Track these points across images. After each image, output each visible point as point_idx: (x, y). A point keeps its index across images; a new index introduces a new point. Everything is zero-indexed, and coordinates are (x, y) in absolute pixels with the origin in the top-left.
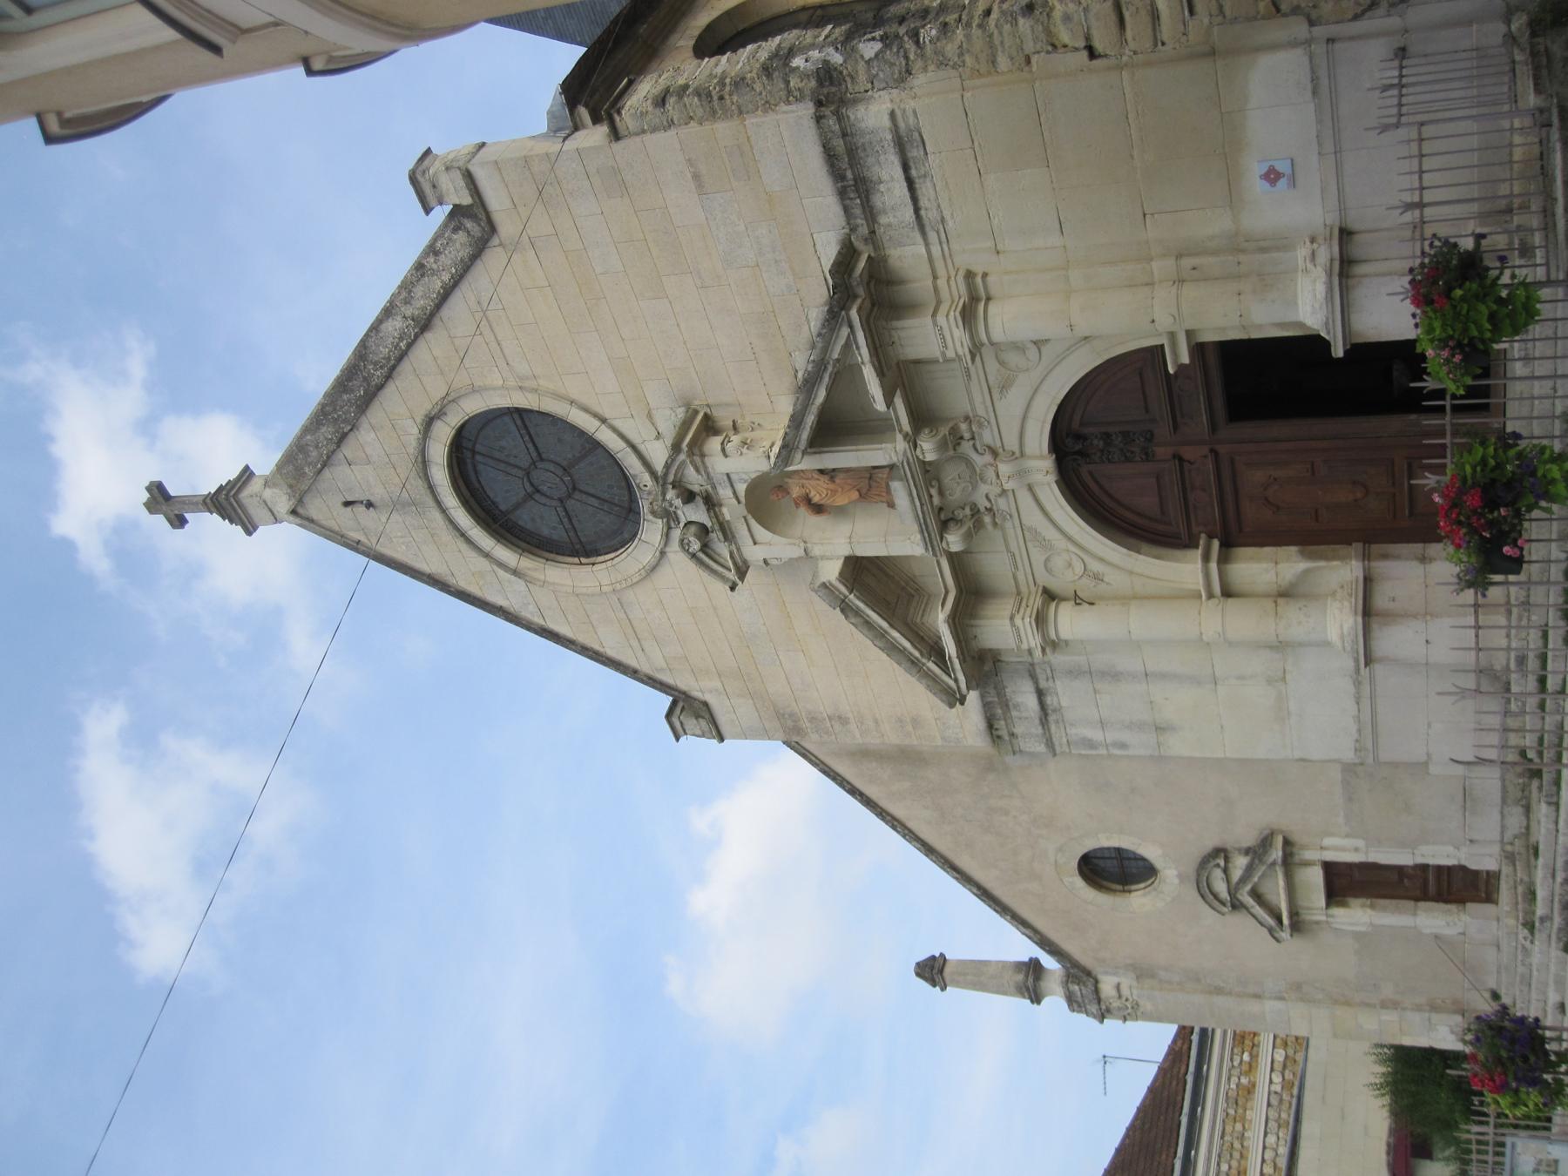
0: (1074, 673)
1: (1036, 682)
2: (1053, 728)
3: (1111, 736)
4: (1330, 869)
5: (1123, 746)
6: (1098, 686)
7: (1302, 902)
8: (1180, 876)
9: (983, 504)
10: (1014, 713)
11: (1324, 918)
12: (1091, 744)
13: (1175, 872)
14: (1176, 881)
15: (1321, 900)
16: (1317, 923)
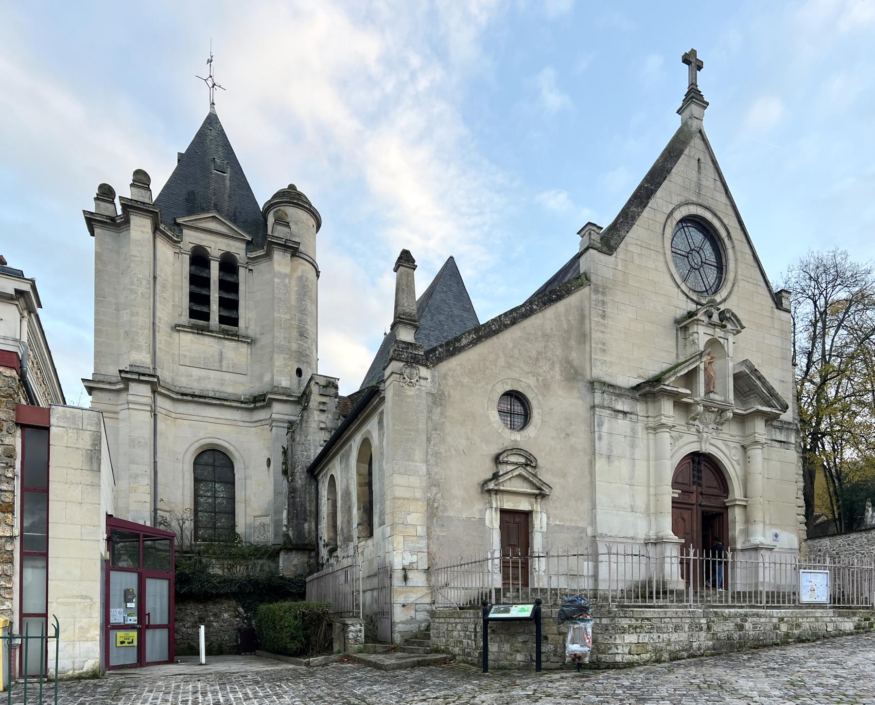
0: (633, 430)
1: (631, 413)
2: (609, 412)
3: (605, 436)
4: (527, 515)
5: (600, 438)
6: (628, 438)
7: (505, 497)
8: (516, 441)
9: (697, 422)
10: (614, 398)
11: (494, 506)
12: (600, 425)
13: (519, 439)
14: (513, 438)
15: (508, 506)
16: (490, 503)
